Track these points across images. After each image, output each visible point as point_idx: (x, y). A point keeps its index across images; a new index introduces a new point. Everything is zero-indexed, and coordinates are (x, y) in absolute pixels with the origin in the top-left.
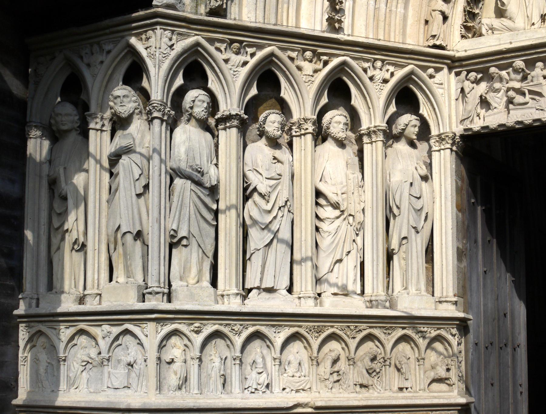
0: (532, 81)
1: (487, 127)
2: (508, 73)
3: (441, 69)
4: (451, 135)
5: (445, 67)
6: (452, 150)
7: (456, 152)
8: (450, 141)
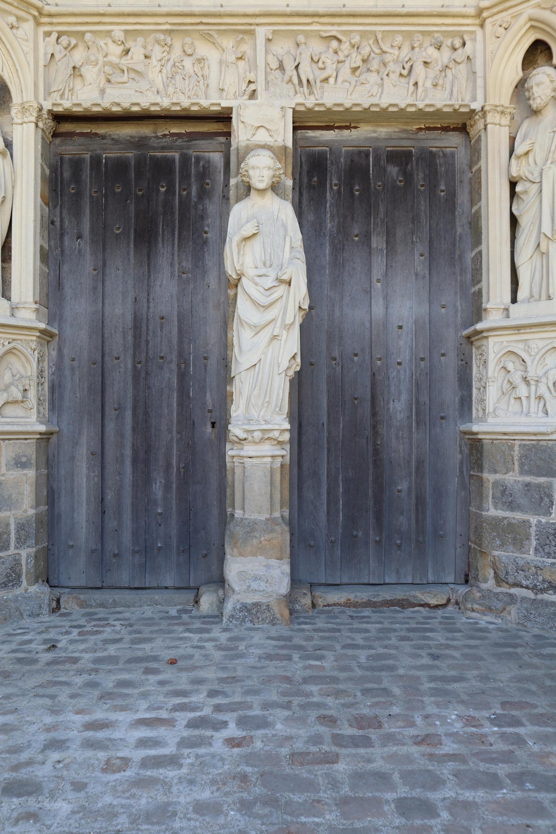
0: (132, 58)
1: (79, 105)
2: (106, 44)
3: (26, 20)
4: (36, 105)
5: (31, 18)
6: (37, 126)
7: (43, 130)
8: (35, 114)
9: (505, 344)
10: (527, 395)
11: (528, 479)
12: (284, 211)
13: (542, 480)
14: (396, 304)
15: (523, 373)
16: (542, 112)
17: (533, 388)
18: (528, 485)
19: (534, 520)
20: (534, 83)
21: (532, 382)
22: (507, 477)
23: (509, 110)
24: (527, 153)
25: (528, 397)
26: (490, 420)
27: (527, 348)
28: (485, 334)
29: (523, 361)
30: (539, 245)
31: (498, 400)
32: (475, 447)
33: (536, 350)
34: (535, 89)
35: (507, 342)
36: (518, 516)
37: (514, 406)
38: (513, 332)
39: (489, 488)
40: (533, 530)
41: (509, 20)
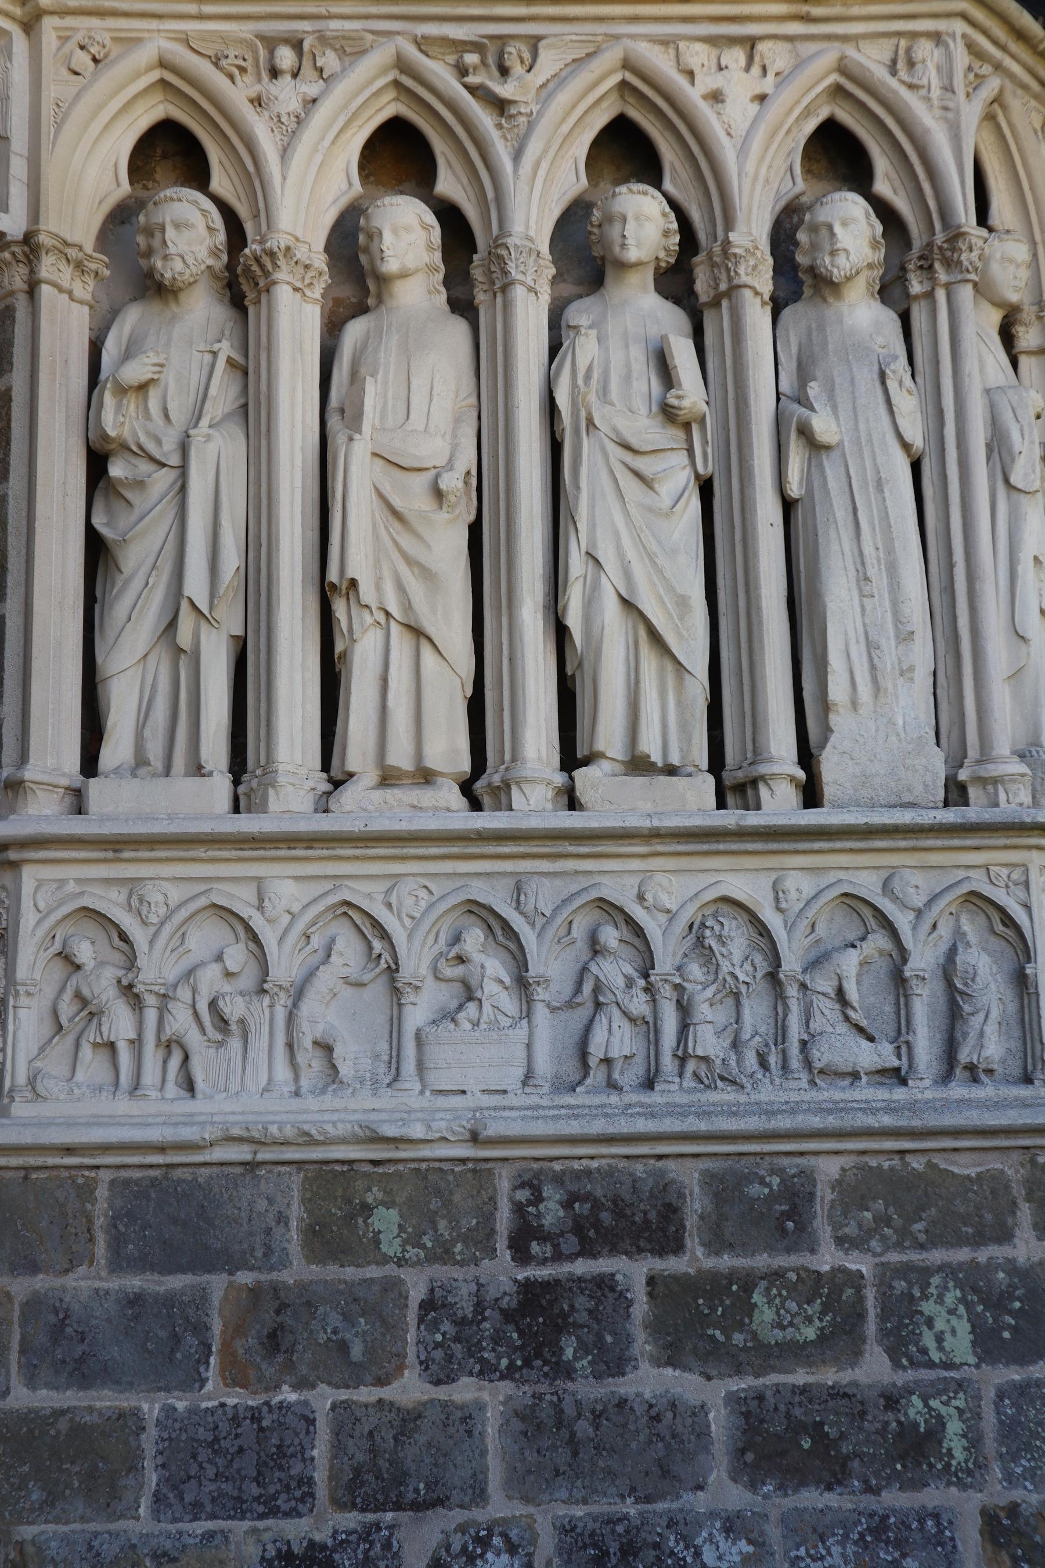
9: (71, 887)
10: (132, 1035)
11: (135, 1283)
13: (177, 1282)
15: (120, 973)
16: (182, 296)
17: (151, 1016)
18: (135, 1301)
19: (151, 1408)
20: (168, 220)
21: (150, 1000)
22: (70, 1281)
23: (93, 266)
24: (143, 388)
25: (137, 1044)
26: (20, 1109)
27: (135, 902)
28: (13, 855)
29: (123, 937)
30: (172, 625)
31: (42, 1049)
33: (162, 911)
34: (170, 233)
35: (79, 881)
36: (105, 1399)
37: (92, 1066)
38: (101, 855)
39: (10, 1323)
40: (149, 1441)
41: (108, 42)
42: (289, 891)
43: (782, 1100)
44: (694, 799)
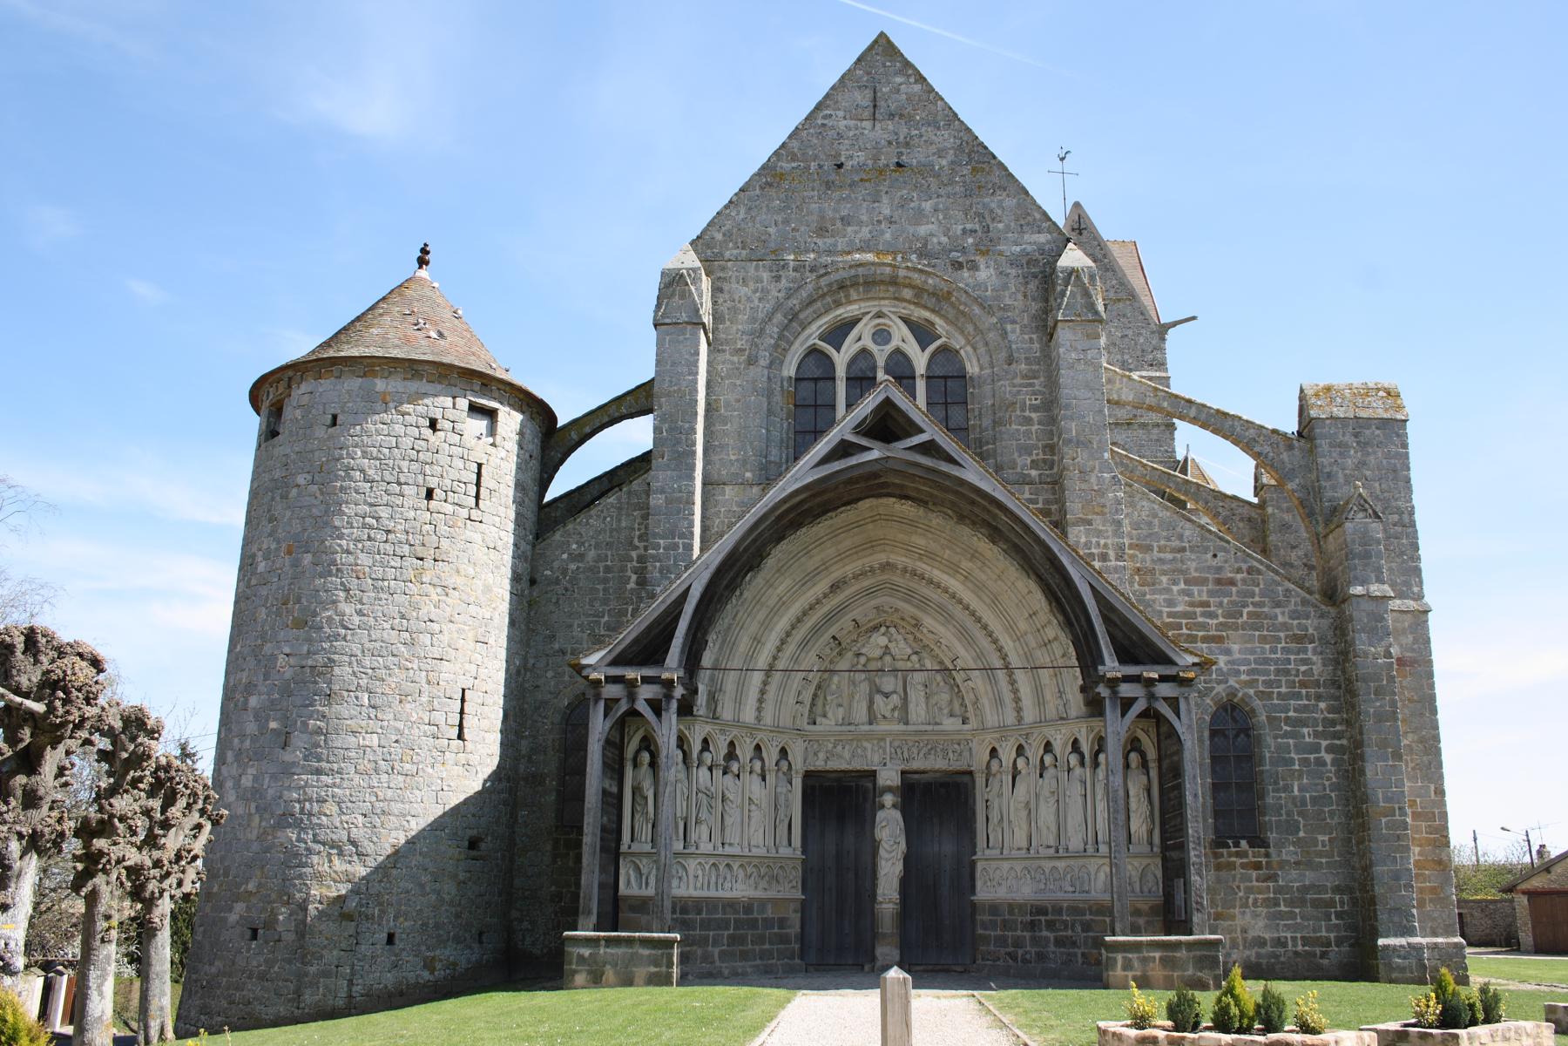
12: (897, 815)
14: (944, 847)
32: (973, 905)
42: (1006, 865)
43: (1060, 895)
44: (1052, 851)
